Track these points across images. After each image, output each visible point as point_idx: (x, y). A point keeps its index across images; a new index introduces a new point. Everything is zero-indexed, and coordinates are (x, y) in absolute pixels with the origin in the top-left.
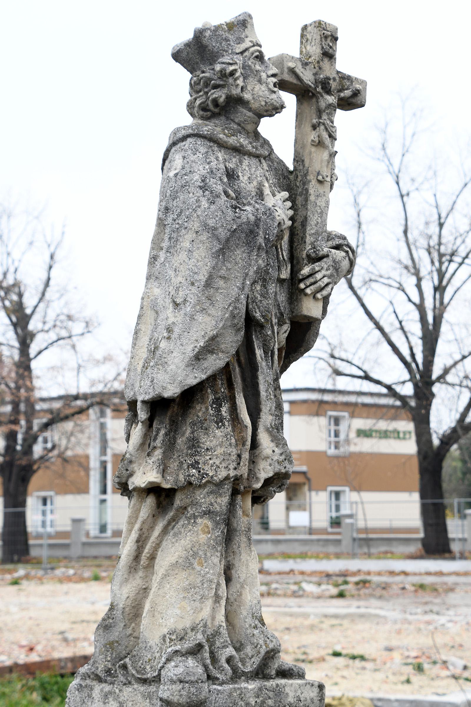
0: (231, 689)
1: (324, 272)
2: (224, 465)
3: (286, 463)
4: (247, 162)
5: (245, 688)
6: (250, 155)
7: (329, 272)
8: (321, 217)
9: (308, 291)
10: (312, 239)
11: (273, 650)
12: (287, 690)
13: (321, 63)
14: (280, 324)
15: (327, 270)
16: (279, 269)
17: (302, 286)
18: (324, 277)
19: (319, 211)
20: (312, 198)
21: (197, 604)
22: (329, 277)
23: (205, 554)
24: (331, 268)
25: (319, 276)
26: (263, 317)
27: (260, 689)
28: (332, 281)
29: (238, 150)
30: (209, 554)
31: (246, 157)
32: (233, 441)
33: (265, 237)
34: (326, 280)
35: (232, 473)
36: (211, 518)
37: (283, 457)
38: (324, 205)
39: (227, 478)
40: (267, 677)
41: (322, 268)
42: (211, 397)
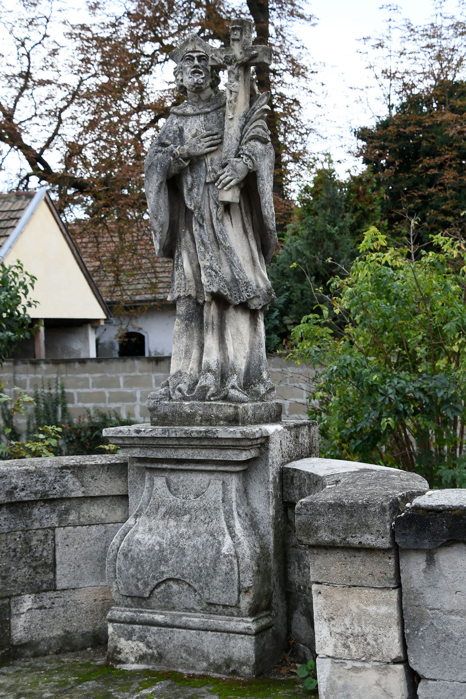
1: (226, 174)
2: (178, 290)
3: (211, 287)
6: (193, 115)
7: (229, 173)
9: (219, 187)
10: (226, 155)
11: (204, 387)
14: (218, 207)
15: (228, 172)
16: (206, 178)
17: (216, 184)
20: (226, 130)
21: (178, 362)
22: (231, 176)
25: (221, 178)
26: (195, 207)
29: (185, 115)
32: (183, 276)
35: (182, 294)
36: (179, 318)
37: (209, 283)
39: (179, 298)
40: (203, 399)
42: (176, 254)
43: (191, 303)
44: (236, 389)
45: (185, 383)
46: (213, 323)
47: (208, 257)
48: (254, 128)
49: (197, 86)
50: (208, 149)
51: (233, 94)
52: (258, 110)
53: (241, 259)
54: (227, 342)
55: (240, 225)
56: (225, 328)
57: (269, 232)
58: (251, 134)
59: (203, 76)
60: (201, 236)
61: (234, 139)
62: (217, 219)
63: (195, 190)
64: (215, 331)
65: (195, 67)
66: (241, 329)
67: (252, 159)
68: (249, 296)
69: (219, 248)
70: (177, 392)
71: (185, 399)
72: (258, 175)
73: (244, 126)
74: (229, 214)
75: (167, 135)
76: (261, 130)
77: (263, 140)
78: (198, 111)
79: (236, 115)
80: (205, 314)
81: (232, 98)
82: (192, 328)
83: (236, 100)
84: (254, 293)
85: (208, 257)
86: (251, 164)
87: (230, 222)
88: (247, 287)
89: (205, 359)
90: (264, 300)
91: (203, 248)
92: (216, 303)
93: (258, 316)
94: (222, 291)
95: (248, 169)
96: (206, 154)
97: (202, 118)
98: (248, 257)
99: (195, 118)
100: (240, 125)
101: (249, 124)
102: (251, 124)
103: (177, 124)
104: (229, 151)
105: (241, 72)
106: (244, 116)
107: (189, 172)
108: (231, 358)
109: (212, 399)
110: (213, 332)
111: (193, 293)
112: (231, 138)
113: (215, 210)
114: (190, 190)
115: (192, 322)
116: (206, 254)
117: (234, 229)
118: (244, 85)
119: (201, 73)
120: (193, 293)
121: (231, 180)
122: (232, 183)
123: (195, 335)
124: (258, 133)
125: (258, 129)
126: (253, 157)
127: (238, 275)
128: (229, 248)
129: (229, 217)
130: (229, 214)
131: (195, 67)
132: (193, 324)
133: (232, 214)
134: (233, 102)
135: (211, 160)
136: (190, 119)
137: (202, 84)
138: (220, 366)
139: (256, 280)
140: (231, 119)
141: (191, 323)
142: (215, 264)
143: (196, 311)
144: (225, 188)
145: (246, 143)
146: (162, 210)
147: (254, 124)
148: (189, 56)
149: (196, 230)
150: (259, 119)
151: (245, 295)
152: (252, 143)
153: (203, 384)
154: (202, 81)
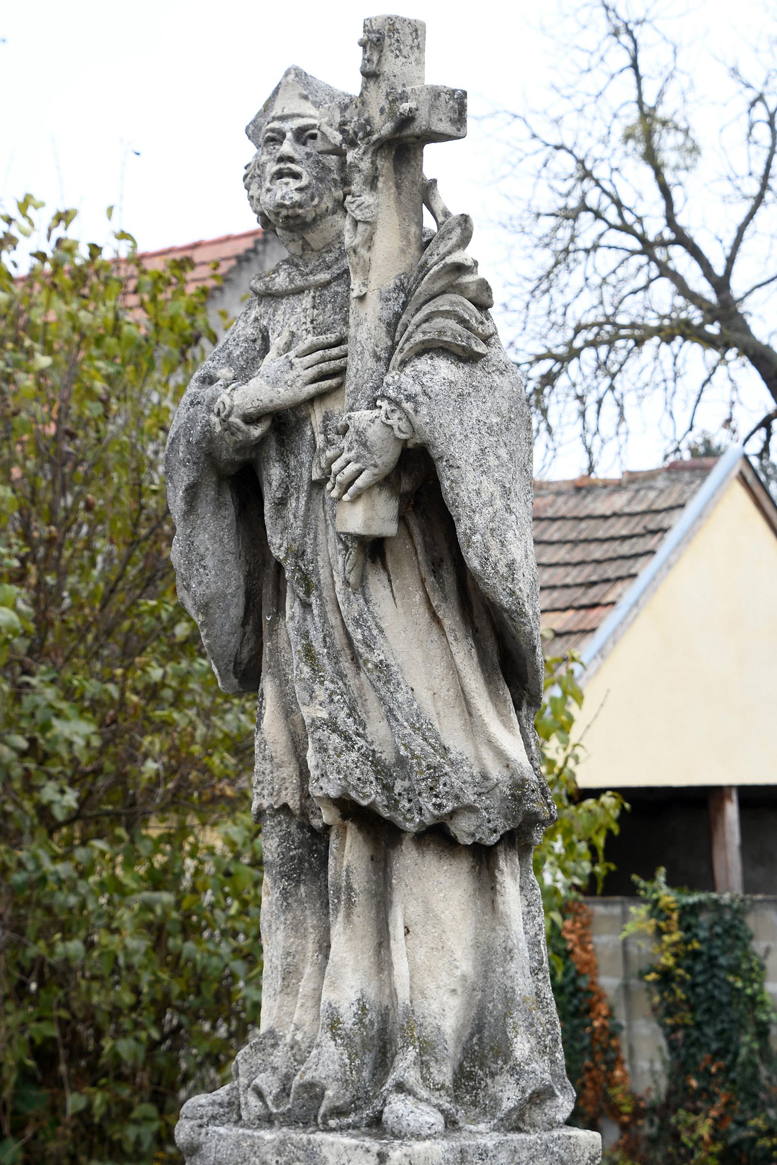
0: (239, 1136)
1: (346, 456)
4: (282, 307)
5: (259, 1137)
7: (352, 454)
8: (361, 359)
12: (325, 1150)
13: (365, 93)
15: (349, 450)
18: (348, 463)
19: (359, 350)
23: (270, 926)
24: (355, 444)
25: (335, 467)
27: (283, 1143)
28: (363, 464)
30: (274, 927)
31: (284, 301)
33: (189, 441)
34: (352, 467)
35: (266, 805)
38: (366, 336)
41: (342, 451)
43: (293, 828)
44: (410, 1092)
45: (275, 1069)
46: (349, 888)
47: (321, 694)
48: (427, 319)
49: (284, 212)
50: (312, 388)
51: (361, 227)
52: (435, 268)
53: (424, 696)
54: (392, 942)
55: (418, 597)
56: (391, 902)
57: (505, 615)
58: (419, 337)
59: (304, 182)
60: (306, 635)
61: (367, 353)
62: (346, 583)
63: (292, 503)
64: (358, 910)
65: (281, 159)
66: (438, 907)
67: (403, 410)
68: (439, 806)
69: (358, 668)
70: (253, 1100)
71: (268, 1120)
72: (434, 453)
73: (398, 316)
74: (385, 568)
75: (230, 354)
76: (452, 323)
77: (460, 352)
78: (299, 282)
79: (372, 286)
80: (331, 861)
81: (358, 240)
82: (300, 902)
83: (369, 242)
84: (457, 797)
85: (321, 694)
86: (404, 425)
87: (388, 590)
88: (436, 780)
89: (327, 996)
90: (506, 819)
91: (306, 669)
92: (360, 829)
93: (496, 866)
94: (353, 794)
95: (397, 439)
96: (311, 400)
97: (307, 301)
98: (447, 692)
99: (293, 300)
100: (387, 314)
101: (410, 308)
102: (418, 310)
103: (256, 320)
104: (357, 389)
105: (385, 165)
106: (400, 288)
107: (273, 454)
108: (403, 995)
109: (332, 1123)
110: (348, 916)
111: (294, 803)
112: (362, 353)
113: (340, 559)
114: (281, 503)
115: (298, 882)
116: (316, 687)
117: (401, 610)
118: (398, 201)
119: (296, 176)
120: (294, 803)
121: (360, 472)
122: (359, 482)
123: (311, 921)
124: (441, 332)
125: (439, 322)
126: (408, 406)
127: (407, 747)
128: (382, 667)
129: (384, 577)
130: (385, 568)
131: (281, 159)
132: (302, 889)
133: (390, 565)
134: (362, 251)
135: (326, 418)
136: (285, 305)
137: (300, 205)
138: (372, 1016)
139: (479, 759)
140: (362, 298)
141: (297, 886)
142: (342, 715)
143: (311, 852)
144: (346, 497)
145: (404, 363)
146: (209, 562)
147: (426, 310)
148: (273, 130)
149: (292, 618)
150: (443, 292)
151: (428, 804)
152: (423, 364)
153: (308, 1077)
154: (297, 197)
